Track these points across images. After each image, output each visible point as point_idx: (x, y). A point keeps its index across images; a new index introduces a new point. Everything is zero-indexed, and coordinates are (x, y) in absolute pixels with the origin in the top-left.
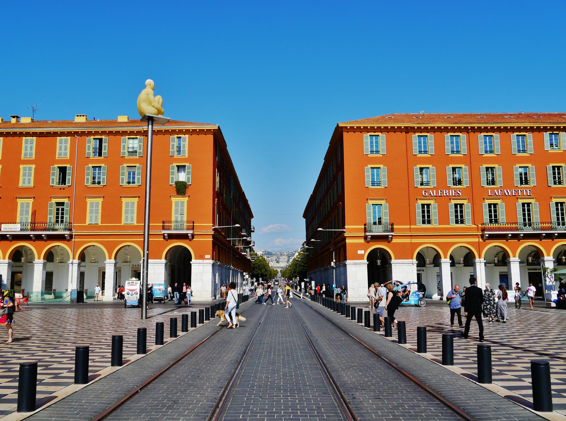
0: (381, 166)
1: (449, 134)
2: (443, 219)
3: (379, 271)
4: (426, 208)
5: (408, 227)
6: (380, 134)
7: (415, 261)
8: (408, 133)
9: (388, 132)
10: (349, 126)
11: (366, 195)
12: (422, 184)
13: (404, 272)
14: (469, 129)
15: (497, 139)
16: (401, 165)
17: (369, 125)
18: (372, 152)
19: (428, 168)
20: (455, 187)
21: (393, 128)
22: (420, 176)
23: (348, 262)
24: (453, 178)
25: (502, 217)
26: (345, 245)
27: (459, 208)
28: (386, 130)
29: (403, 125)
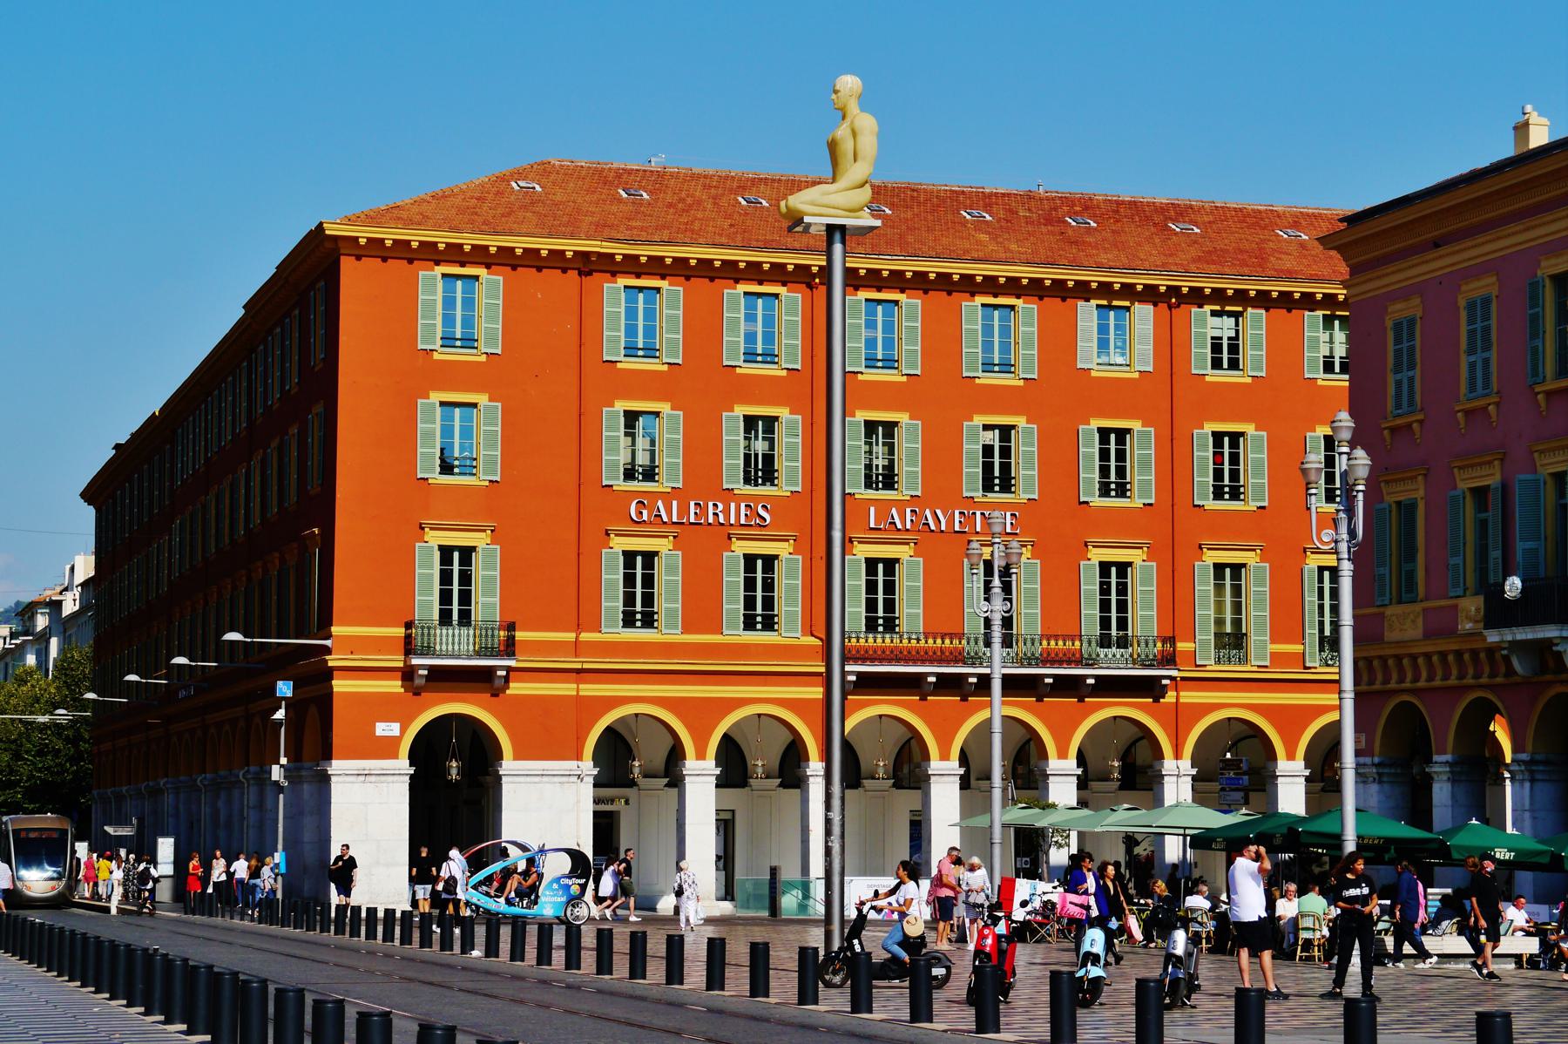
0: (482, 399)
1: (742, 288)
2: (702, 613)
3: (453, 799)
4: (639, 567)
5: (570, 636)
6: (481, 271)
7: (588, 767)
8: (589, 273)
9: (514, 268)
10: (363, 234)
11: (414, 506)
12: (629, 474)
13: (545, 807)
14: (814, 276)
15: (912, 318)
16: (555, 390)
17: (442, 238)
18: (448, 341)
19: (657, 414)
20: (750, 490)
21: (532, 253)
22: (624, 442)
23: (337, 766)
24: (747, 457)
25: (911, 613)
26: (329, 694)
27: (760, 569)
28: (505, 259)
29: (570, 246)
